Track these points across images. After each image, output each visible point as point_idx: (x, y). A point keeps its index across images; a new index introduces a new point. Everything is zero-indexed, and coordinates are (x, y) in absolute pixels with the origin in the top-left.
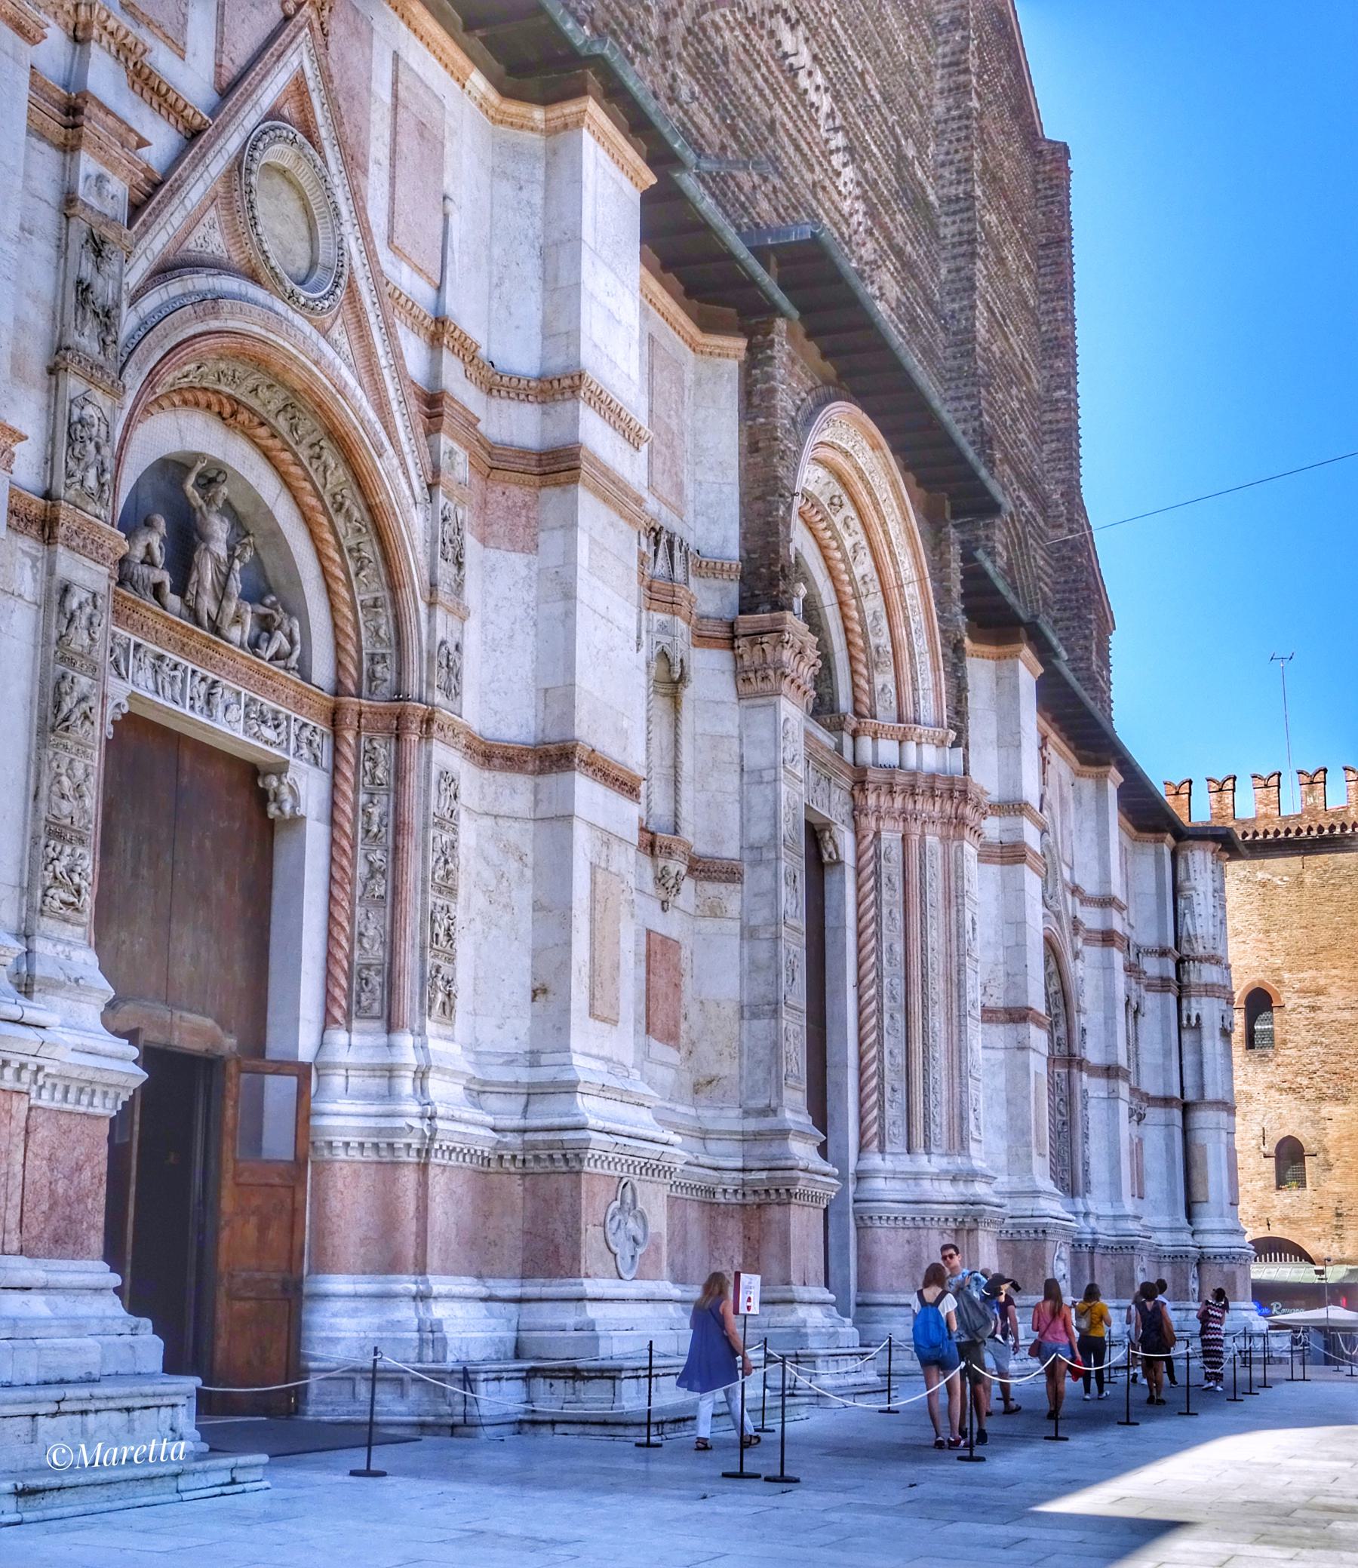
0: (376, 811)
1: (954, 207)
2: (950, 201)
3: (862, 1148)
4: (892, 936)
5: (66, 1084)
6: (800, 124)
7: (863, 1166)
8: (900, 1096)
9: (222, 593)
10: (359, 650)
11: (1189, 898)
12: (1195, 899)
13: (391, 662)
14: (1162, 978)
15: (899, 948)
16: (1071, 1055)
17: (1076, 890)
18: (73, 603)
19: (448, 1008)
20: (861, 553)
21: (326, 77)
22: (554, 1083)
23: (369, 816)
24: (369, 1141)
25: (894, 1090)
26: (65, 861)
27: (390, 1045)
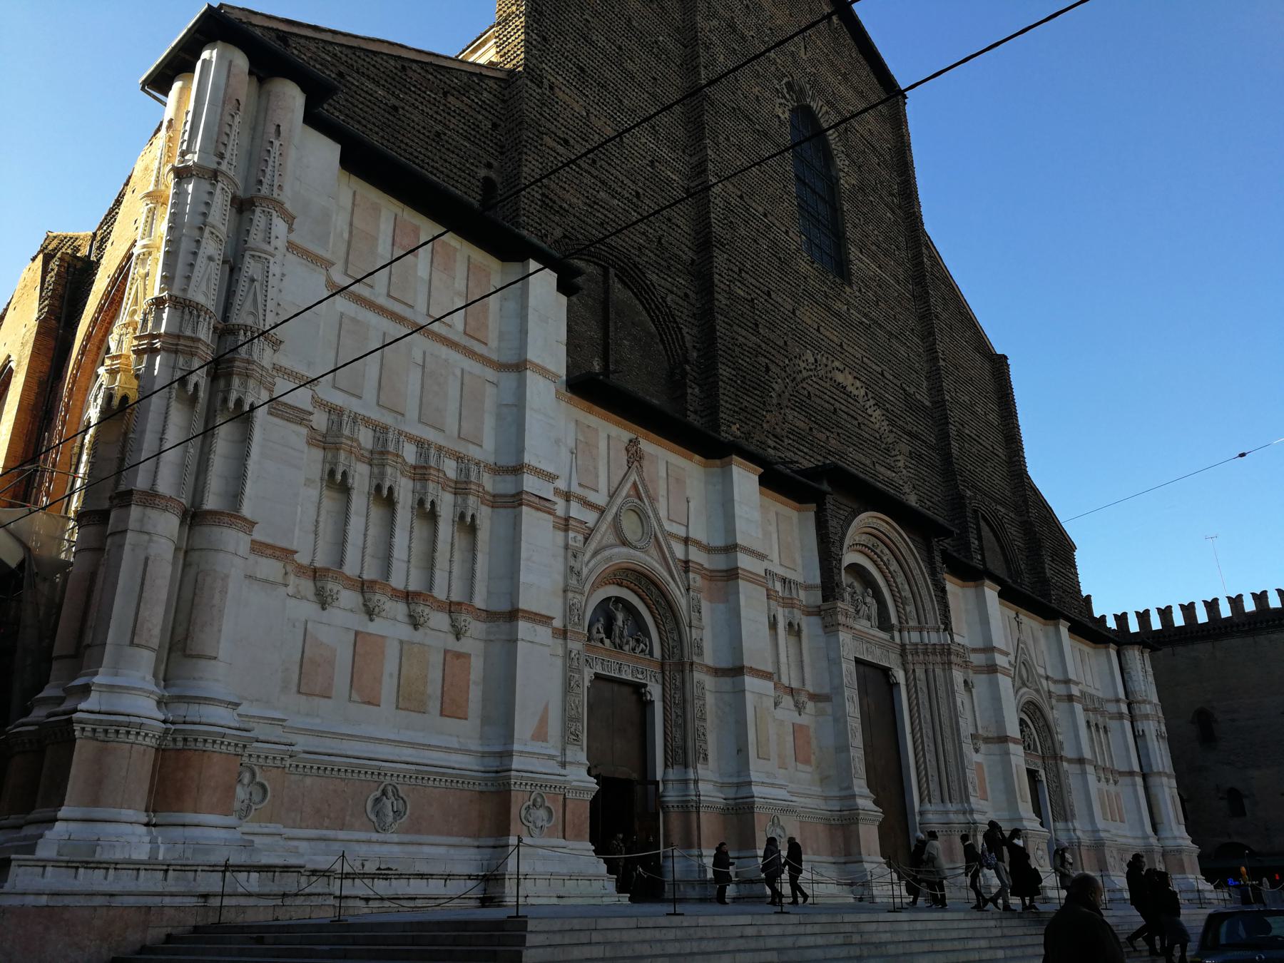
0: (677, 696)
1: (938, 405)
2: (936, 403)
3: (921, 801)
4: (925, 713)
5: (577, 789)
6: (849, 405)
7: (923, 809)
8: (936, 778)
9: (621, 636)
10: (668, 644)
11: (1129, 673)
12: (1133, 673)
13: (679, 647)
14: (1119, 713)
15: (928, 716)
16: (1056, 754)
17: (1047, 678)
18: (573, 655)
19: (706, 758)
20: (891, 562)
21: (642, 480)
22: (745, 782)
23: (675, 698)
24: (680, 805)
25: (932, 776)
26: (574, 727)
27: (686, 772)
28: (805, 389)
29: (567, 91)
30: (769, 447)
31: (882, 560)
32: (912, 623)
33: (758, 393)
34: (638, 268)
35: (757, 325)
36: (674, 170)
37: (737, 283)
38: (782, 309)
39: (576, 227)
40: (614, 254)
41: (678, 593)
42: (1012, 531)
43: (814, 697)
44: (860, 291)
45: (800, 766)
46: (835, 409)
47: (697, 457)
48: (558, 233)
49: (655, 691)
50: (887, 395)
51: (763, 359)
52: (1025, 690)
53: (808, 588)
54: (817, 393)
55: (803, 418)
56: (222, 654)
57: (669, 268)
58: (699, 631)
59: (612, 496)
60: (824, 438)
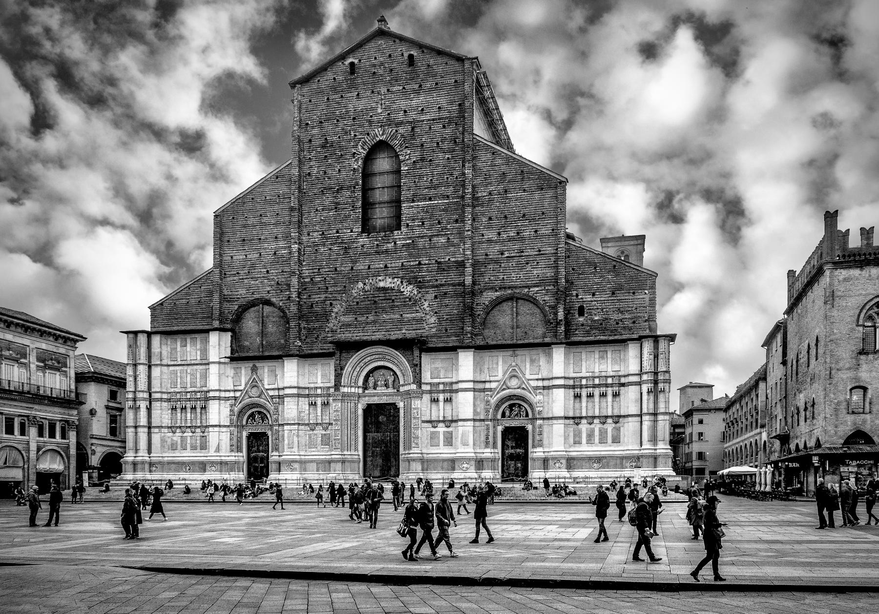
29: (238, 254)
35: (327, 288)
36: (285, 248)
42: (545, 299)
44: (408, 225)
45: (322, 446)
48: (236, 307)
50: (420, 274)
51: (329, 302)
52: (508, 391)
53: (332, 387)
55: (351, 316)
56: (141, 448)
57: (281, 291)
59: (246, 385)
60: (364, 318)
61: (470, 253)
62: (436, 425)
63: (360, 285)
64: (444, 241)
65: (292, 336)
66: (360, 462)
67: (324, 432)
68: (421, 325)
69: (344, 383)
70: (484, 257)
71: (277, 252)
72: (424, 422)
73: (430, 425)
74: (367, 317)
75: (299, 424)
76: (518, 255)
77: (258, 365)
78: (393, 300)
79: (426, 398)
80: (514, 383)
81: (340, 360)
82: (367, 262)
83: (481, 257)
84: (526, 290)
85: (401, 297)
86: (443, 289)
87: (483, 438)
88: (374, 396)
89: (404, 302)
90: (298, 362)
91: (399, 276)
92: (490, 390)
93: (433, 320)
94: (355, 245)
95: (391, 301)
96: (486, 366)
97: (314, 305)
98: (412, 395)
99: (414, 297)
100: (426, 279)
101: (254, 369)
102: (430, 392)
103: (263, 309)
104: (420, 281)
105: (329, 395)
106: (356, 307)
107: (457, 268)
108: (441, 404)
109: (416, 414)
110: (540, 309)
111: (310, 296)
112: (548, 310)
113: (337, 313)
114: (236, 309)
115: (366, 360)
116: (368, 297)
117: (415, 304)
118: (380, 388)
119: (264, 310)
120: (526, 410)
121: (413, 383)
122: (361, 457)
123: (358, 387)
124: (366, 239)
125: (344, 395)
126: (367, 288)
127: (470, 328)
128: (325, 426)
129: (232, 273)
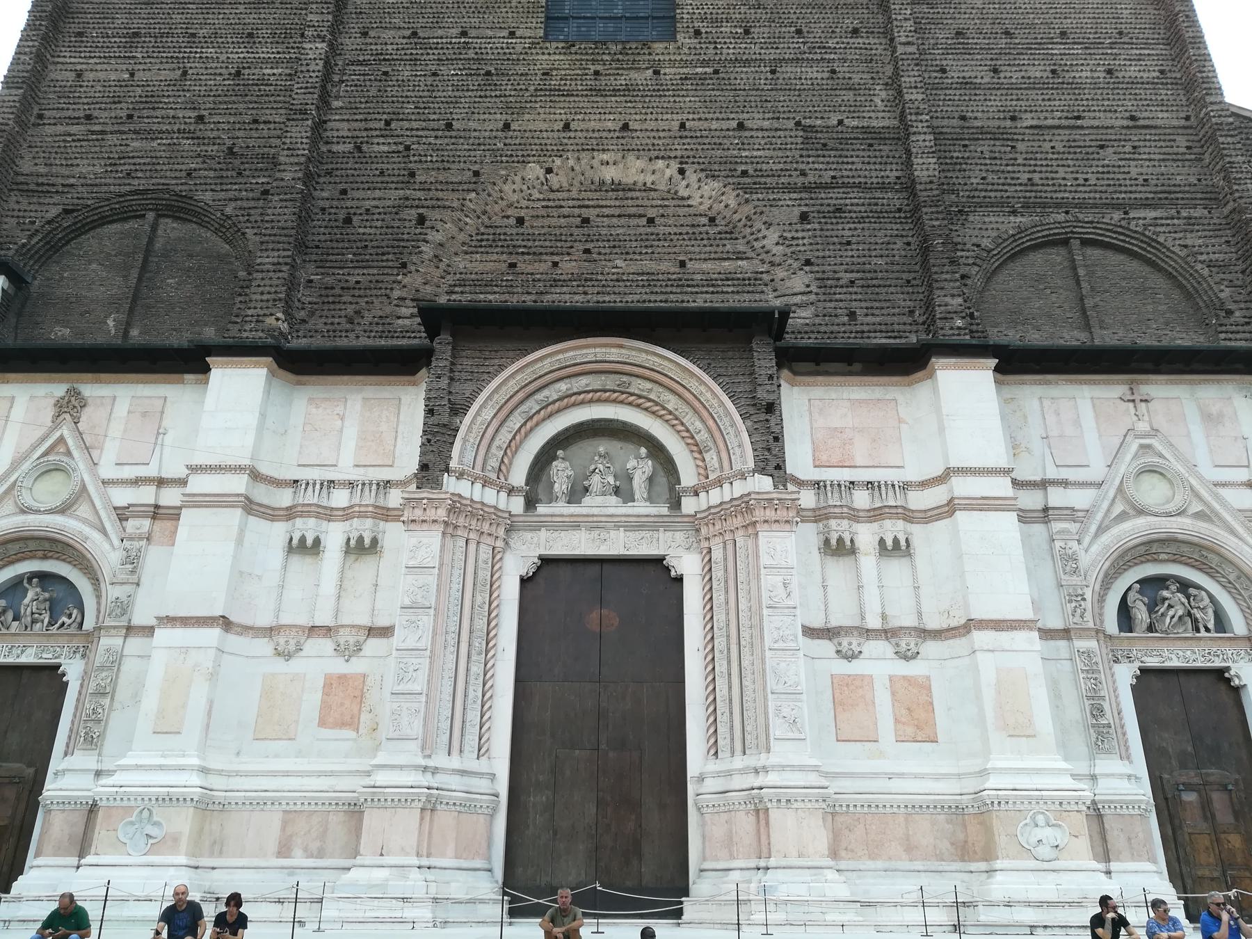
8: (726, 718)
28: (508, 217)
30: (399, 318)
31: (650, 400)
32: (712, 477)
33: (390, 257)
34: (181, 196)
35: (412, 175)
36: (276, 63)
37: (376, 140)
38: (476, 134)
39: (85, 195)
40: (149, 196)
41: (106, 546)
42: (1189, 242)
43: (374, 632)
44: (697, 33)
46: (586, 221)
47: (189, 377)
48: (54, 212)
49: (73, 670)
51: (413, 212)
54: (543, 212)
55: (495, 257)
57: (240, 174)
58: (128, 589)
60: (543, 267)
61: (920, 97)
62: (857, 650)
63: (534, 171)
64: (819, 76)
65: (258, 297)
66: (495, 810)
67: (339, 666)
68: (757, 297)
69: (461, 462)
70: (955, 122)
71: (247, 72)
72: (810, 632)
73: (826, 647)
74: (555, 264)
75: (226, 623)
76: (1072, 122)
77: (96, 390)
78: (651, 221)
79: (810, 533)
80: (1152, 492)
81: (452, 379)
82: (561, 115)
83: (945, 122)
84: (1117, 215)
85: (681, 211)
86: (834, 197)
87: (1075, 710)
88: (576, 526)
89: (693, 225)
90: (269, 383)
91: (672, 154)
92: (1070, 513)
93: (799, 282)
94: (521, 69)
95: (644, 221)
96: (1034, 431)
97: (355, 219)
98: (759, 514)
99: (728, 213)
100: (764, 167)
101: (70, 407)
102: (819, 516)
103: (154, 228)
104: (744, 173)
105: (386, 514)
106: (514, 231)
107: (871, 145)
108: (868, 561)
109: (781, 592)
110: (1170, 276)
111: (344, 192)
112: (1206, 272)
113: (441, 245)
114: (50, 216)
115: (551, 393)
116: (561, 207)
117: (731, 233)
118: (599, 500)
119: (160, 232)
120: (1211, 596)
121: (761, 469)
122: (503, 787)
123: (511, 491)
124: (557, 57)
125: (457, 506)
126: (554, 180)
127: (960, 300)
128: (346, 637)
129: (70, 113)
